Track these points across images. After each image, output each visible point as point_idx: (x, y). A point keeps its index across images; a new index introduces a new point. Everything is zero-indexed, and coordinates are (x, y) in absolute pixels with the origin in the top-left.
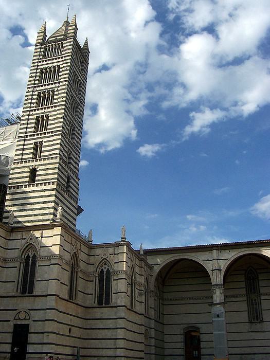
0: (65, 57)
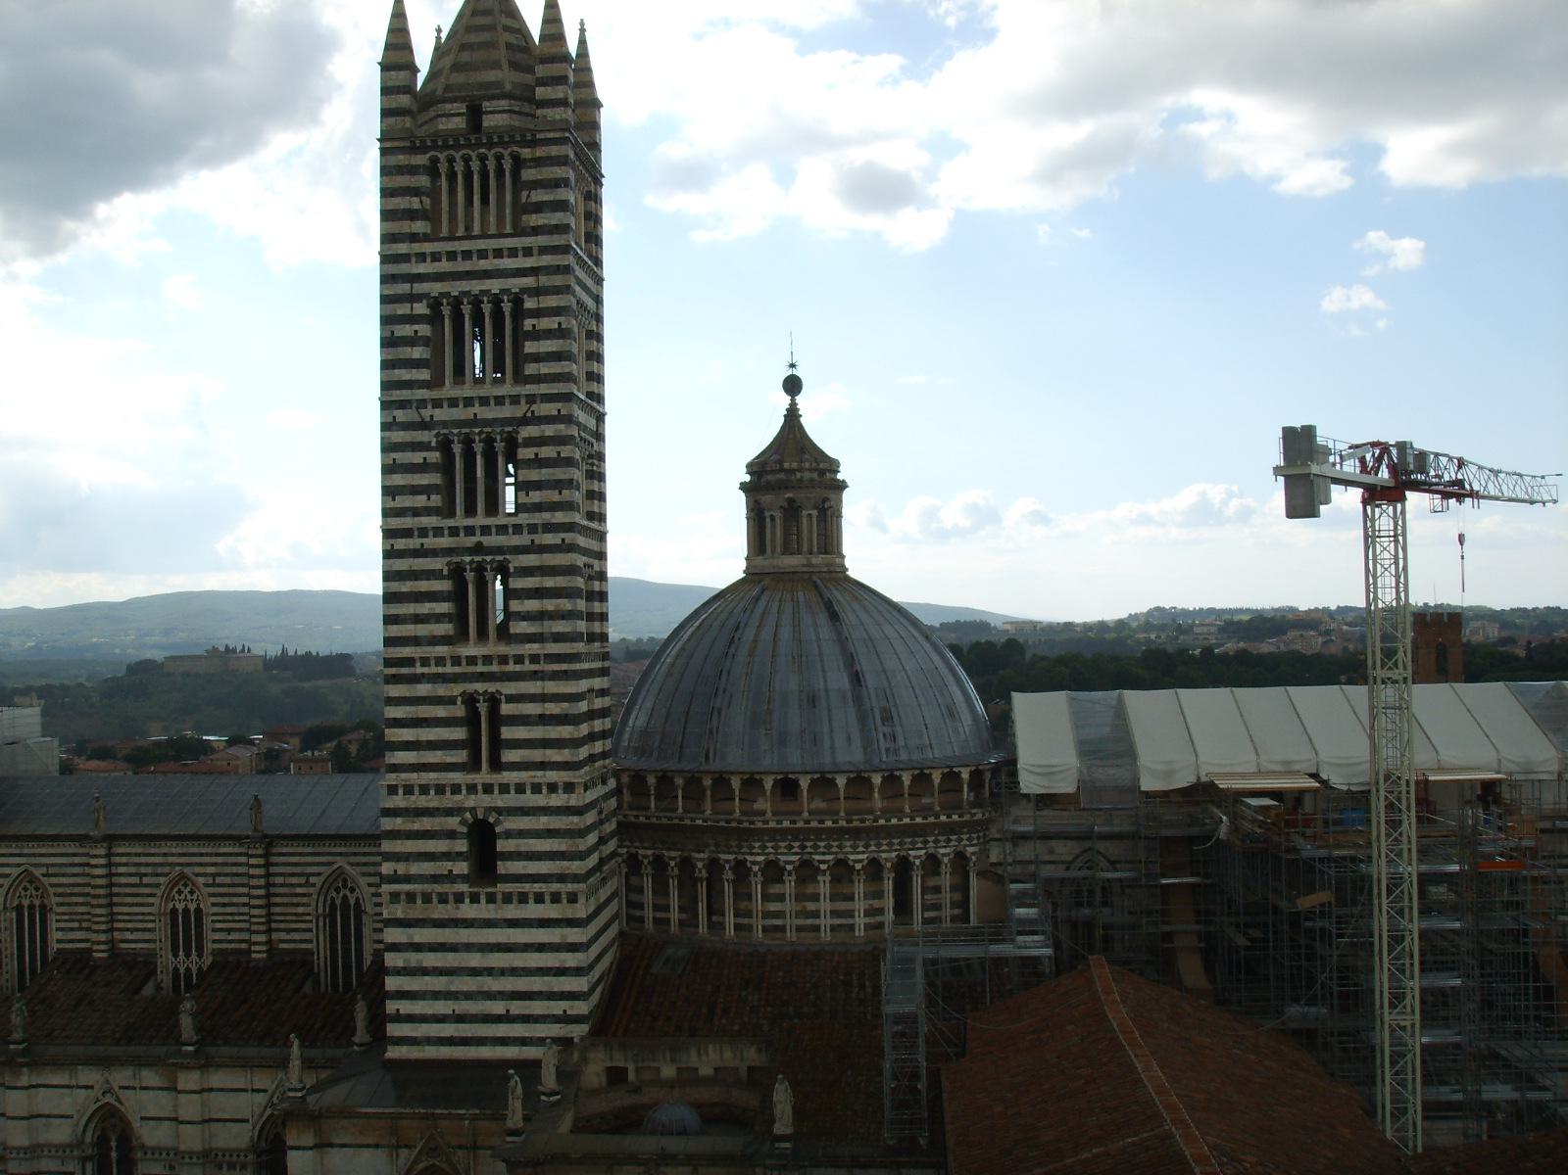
0: (544, 250)
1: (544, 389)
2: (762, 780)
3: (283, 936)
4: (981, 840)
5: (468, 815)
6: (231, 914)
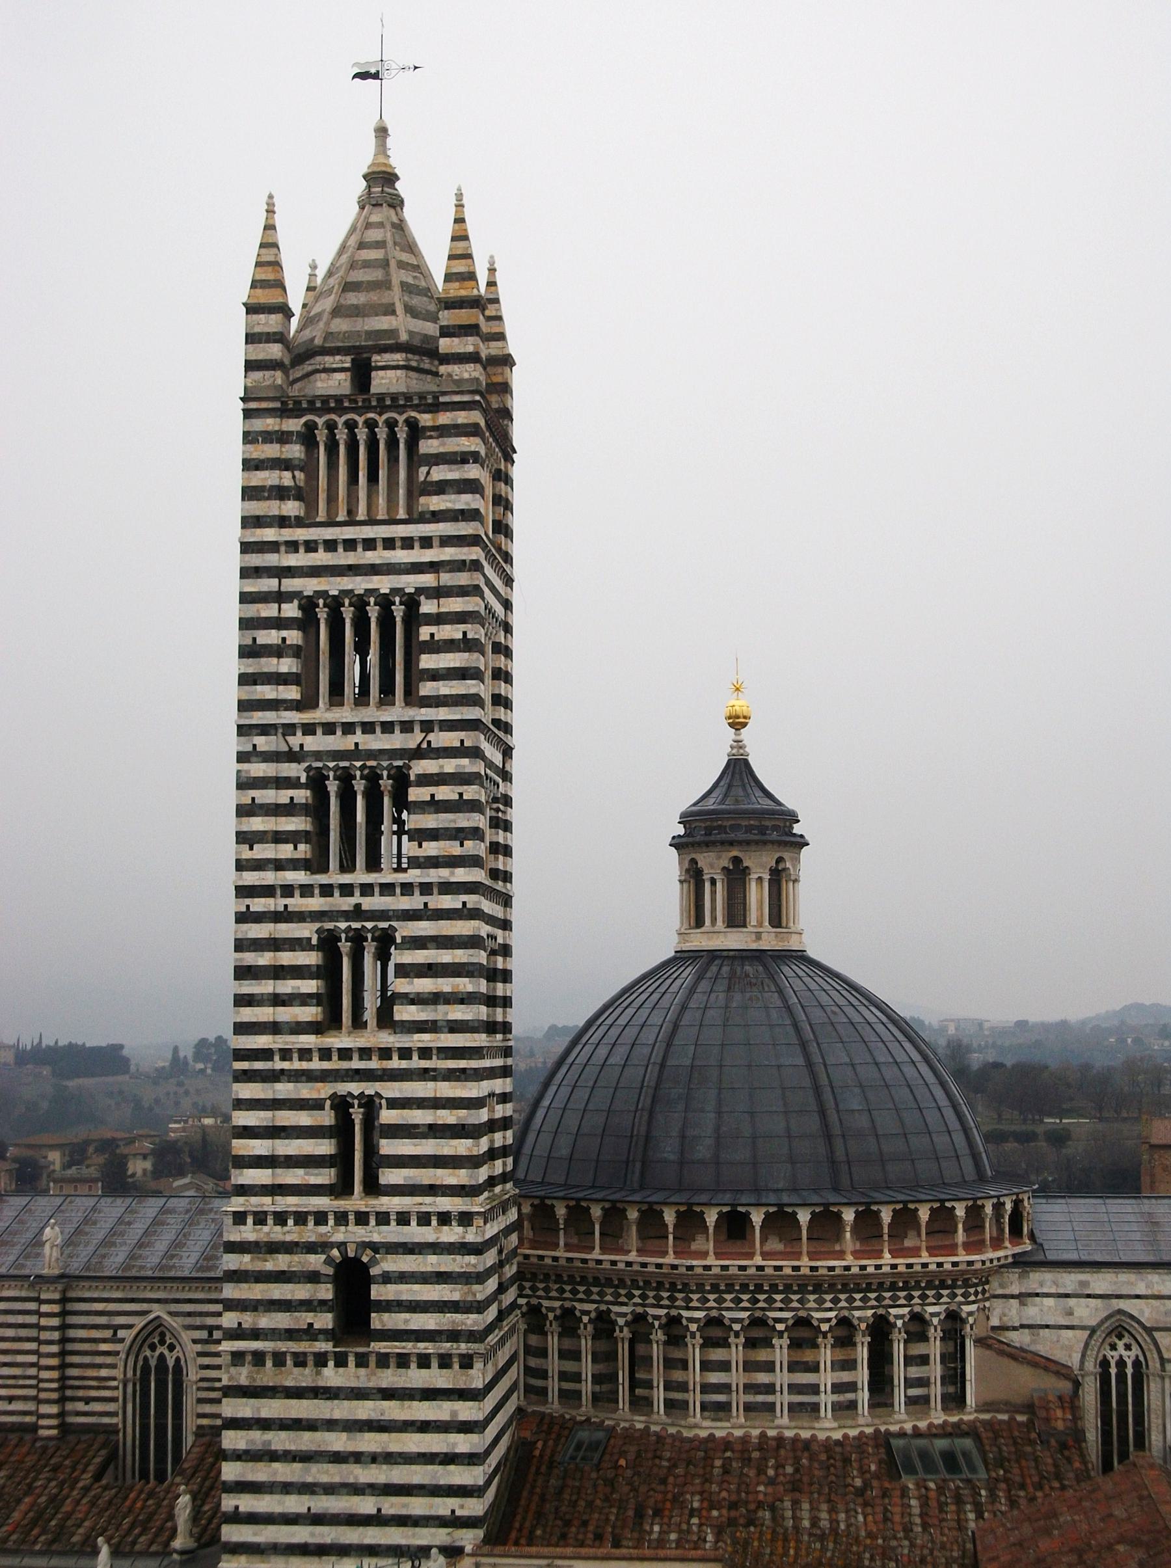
0: (446, 541)
1: (443, 714)
2: (702, 1213)
3: (81, 1406)
4: (980, 1296)
5: (335, 1252)
6: (14, 1377)
